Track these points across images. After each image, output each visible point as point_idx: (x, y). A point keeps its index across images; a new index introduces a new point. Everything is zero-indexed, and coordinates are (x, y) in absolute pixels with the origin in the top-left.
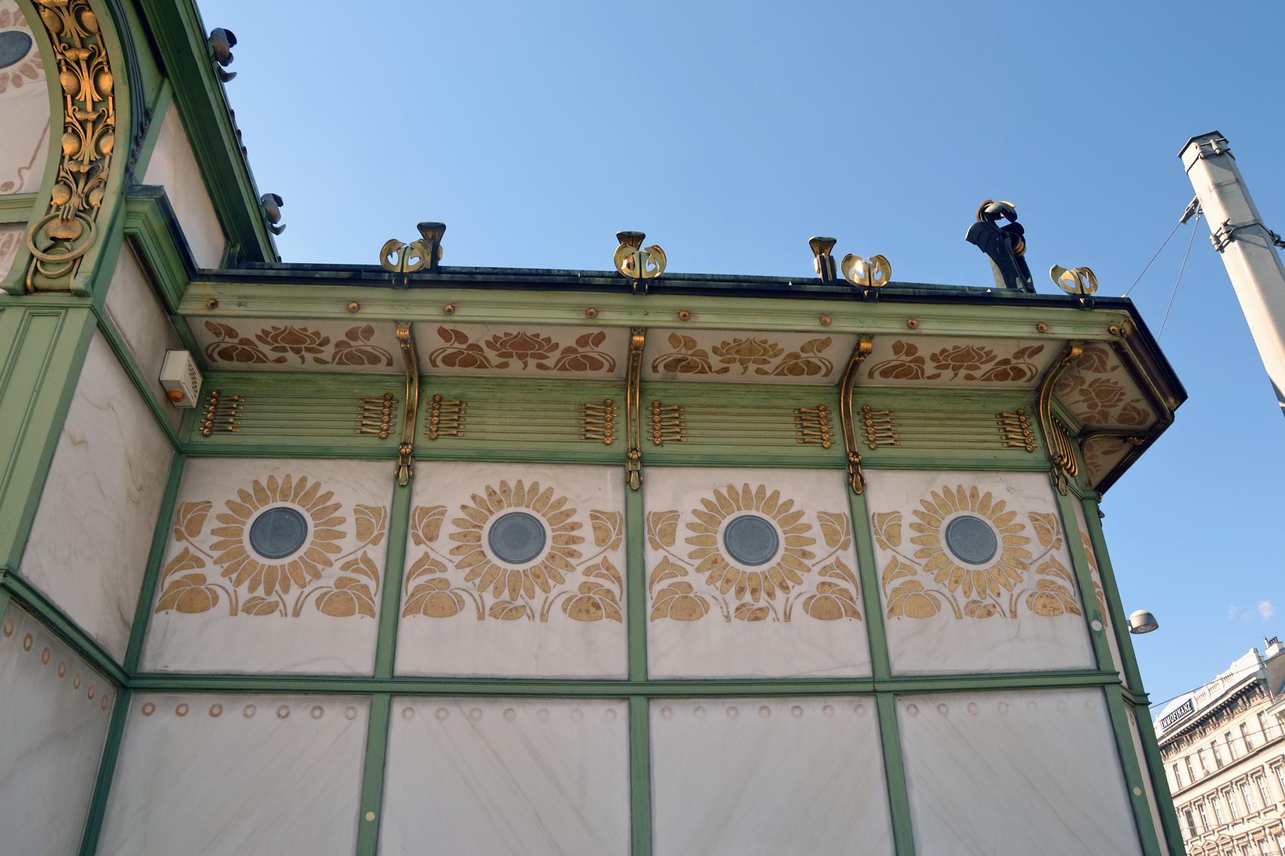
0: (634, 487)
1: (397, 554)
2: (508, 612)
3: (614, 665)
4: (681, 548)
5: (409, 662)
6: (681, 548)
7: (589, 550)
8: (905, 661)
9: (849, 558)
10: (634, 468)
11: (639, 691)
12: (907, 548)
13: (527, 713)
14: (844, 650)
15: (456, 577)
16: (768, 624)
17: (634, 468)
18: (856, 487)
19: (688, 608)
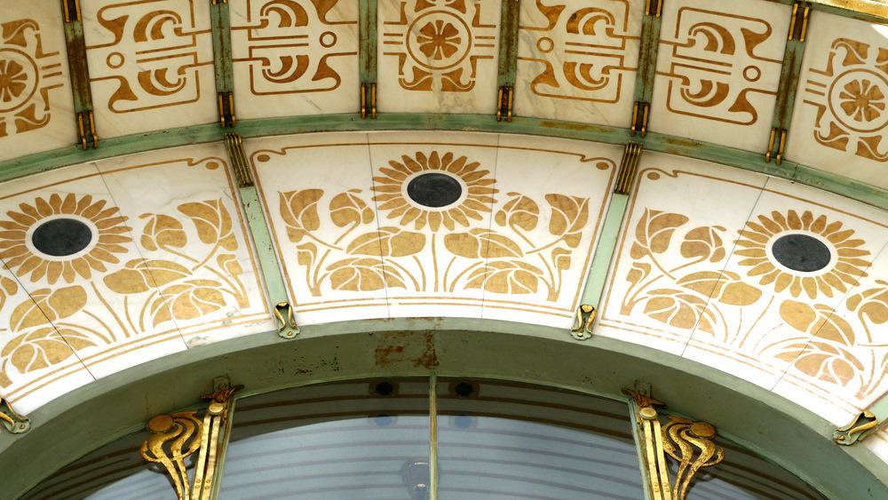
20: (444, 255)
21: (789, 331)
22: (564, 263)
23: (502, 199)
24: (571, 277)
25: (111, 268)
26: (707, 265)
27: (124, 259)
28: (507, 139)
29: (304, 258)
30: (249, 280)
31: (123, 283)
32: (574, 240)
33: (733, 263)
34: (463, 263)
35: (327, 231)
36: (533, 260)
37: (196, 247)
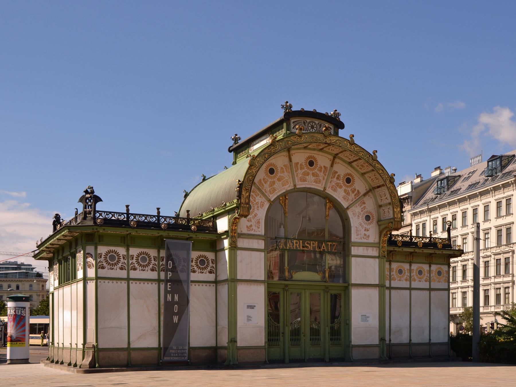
0: (410, 266)
1: (390, 273)
2: (400, 280)
3: (409, 287)
4: (414, 273)
5: (392, 286)
6: (414, 273)
7: (406, 273)
8: (432, 287)
9: (428, 275)
10: (410, 263)
11: (410, 289)
12: (434, 274)
13: (402, 291)
14: (426, 285)
15: (395, 276)
16: (421, 283)
17: (410, 263)
18: (430, 266)
19: (415, 280)
20: (312, 176)
21: (344, 194)
22: (324, 179)
23: (319, 166)
24: (324, 181)
25: (278, 177)
26: (338, 182)
27: (278, 175)
28: (320, 153)
29: (297, 176)
30: (291, 179)
31: (279, 180)
32: (325, 175)
33: (341, 182)
34: (313, 178)
35: (299, 171)
36: (320, 178)
37: (286, 173)
